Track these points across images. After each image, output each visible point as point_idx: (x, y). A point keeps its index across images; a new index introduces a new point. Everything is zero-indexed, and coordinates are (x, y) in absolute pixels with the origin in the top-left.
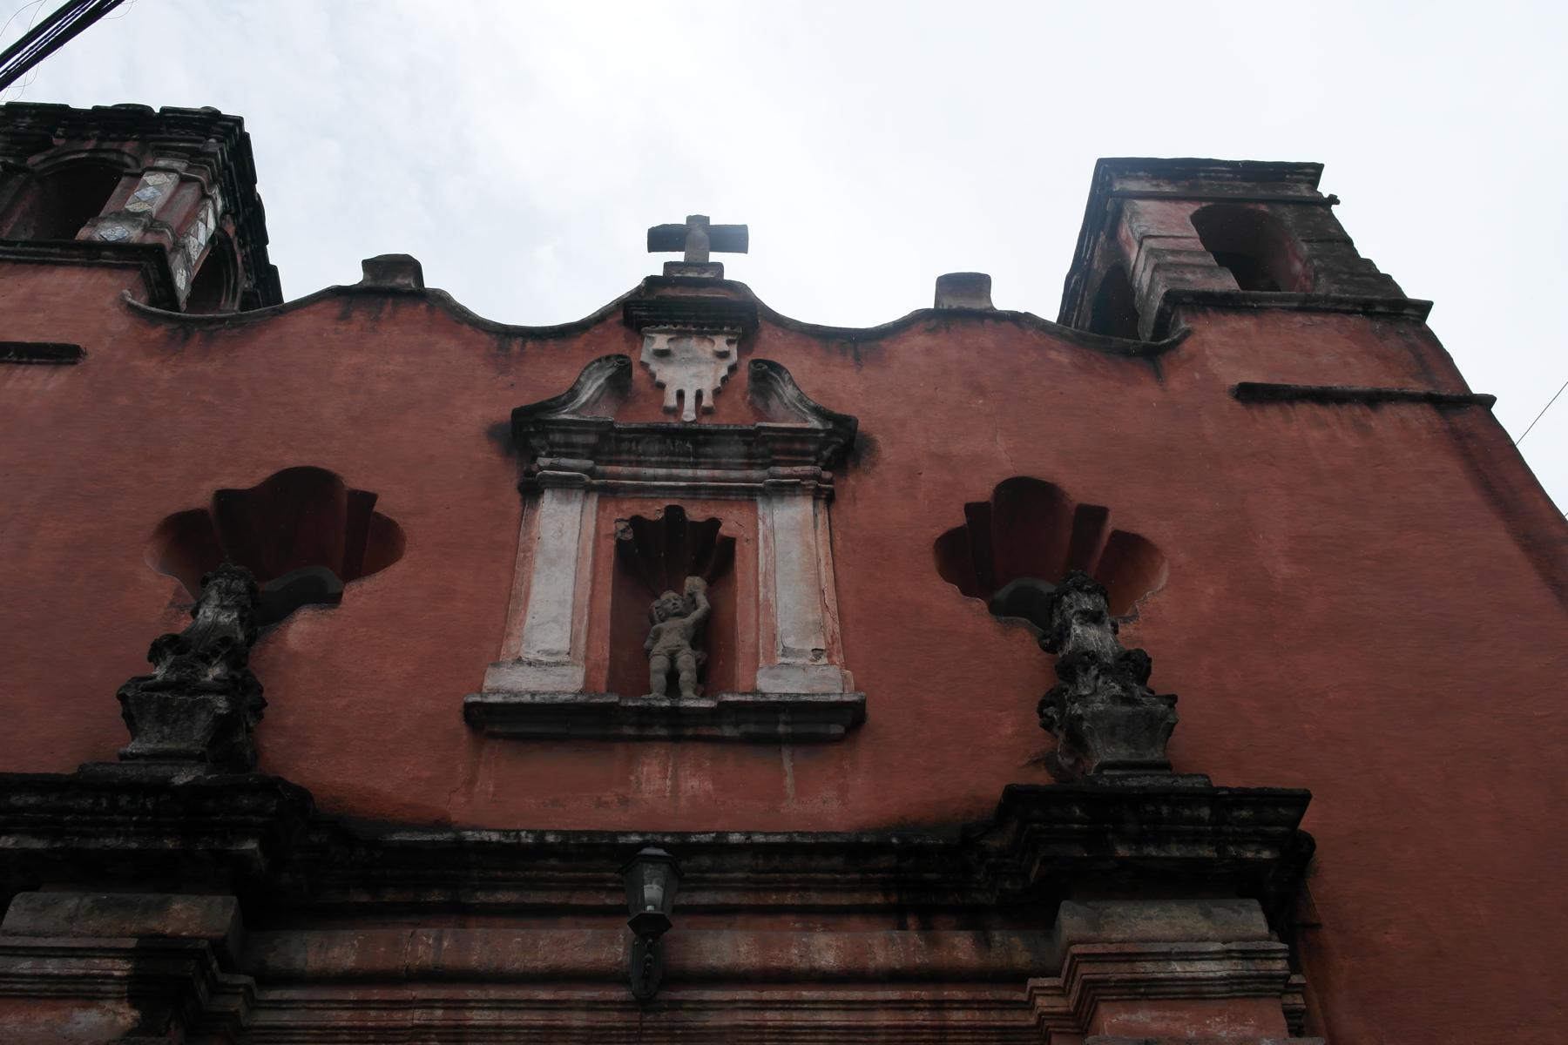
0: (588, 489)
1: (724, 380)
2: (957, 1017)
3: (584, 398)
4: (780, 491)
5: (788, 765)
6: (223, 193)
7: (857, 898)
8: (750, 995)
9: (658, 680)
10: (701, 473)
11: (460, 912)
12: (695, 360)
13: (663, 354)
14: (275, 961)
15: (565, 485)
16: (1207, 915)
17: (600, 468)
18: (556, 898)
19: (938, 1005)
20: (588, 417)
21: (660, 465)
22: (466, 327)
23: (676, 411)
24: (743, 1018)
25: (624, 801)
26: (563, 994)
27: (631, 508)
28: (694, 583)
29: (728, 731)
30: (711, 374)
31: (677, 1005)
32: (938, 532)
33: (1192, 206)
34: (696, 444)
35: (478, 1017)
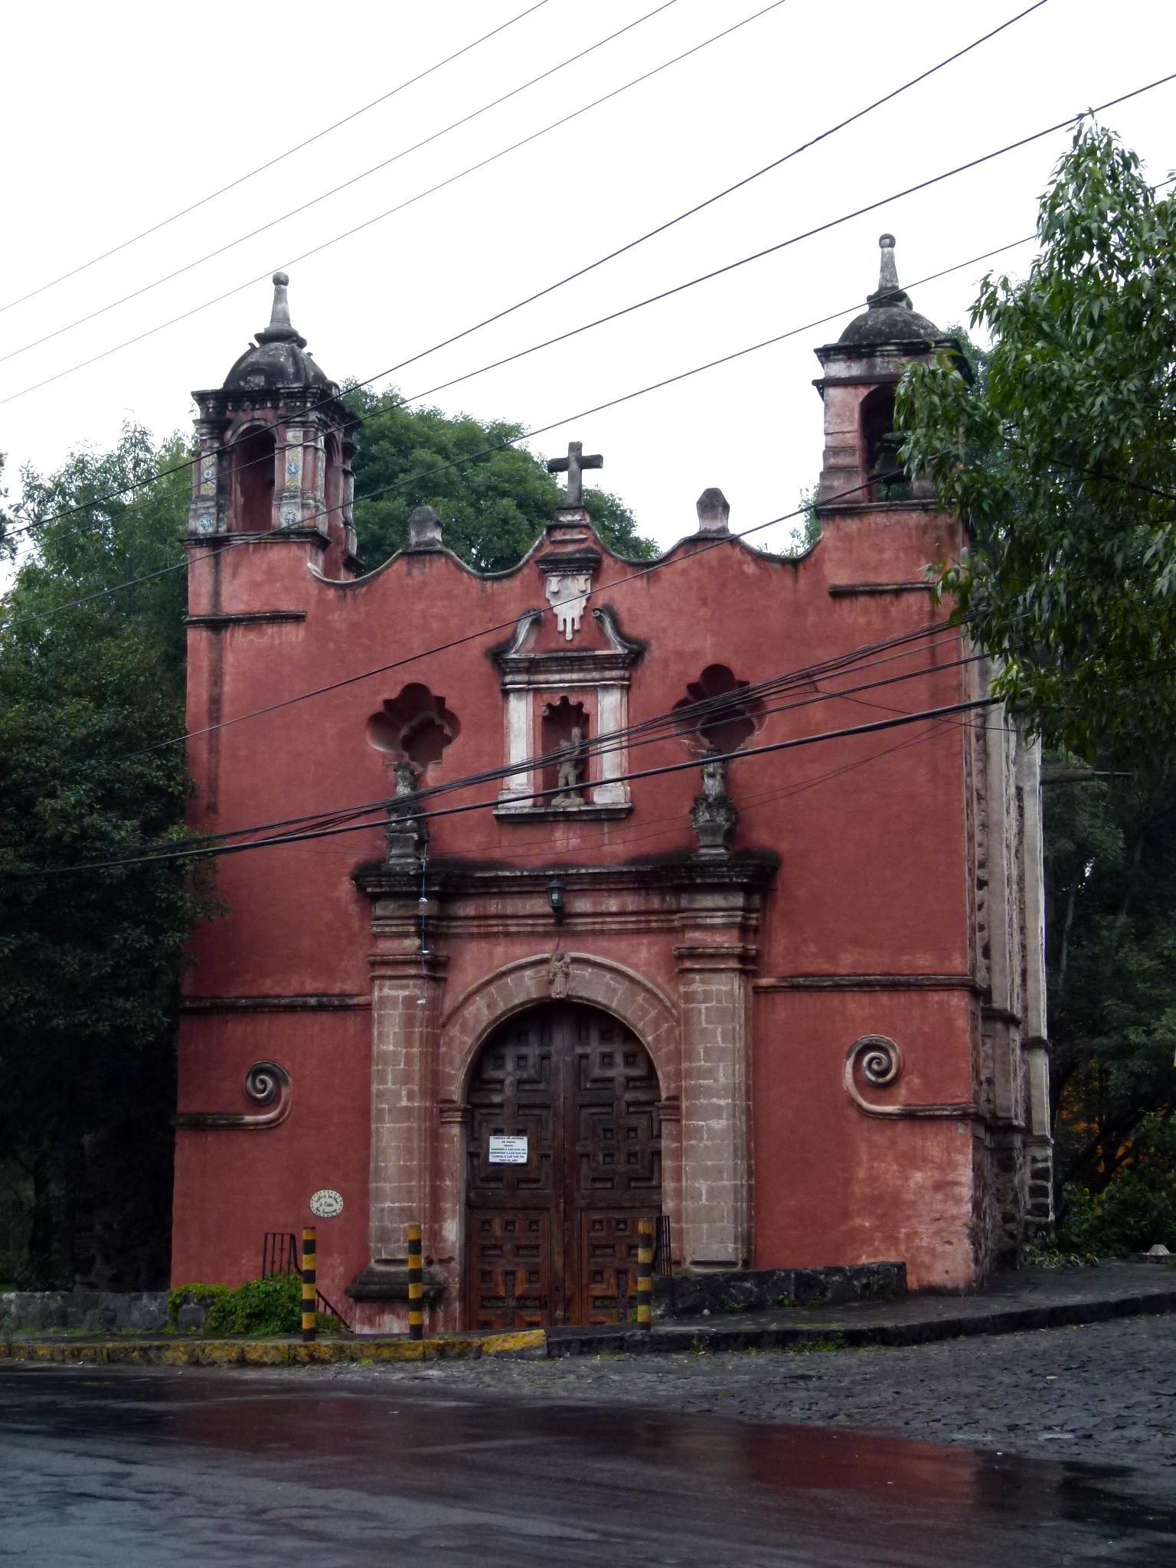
0: (529, 690)
1: (585, 608)
2: (654, 925)
3: (521, 640)
4: (606, 688)
5: (606, 830)
8: (590, 920)
10: (575, 676)
11: (501, 894)
13: (555, 593)
16: (725, 899)
18: (530, 889)
19: (648, 922)
22: (465, 575)
23: (564, 632)
24: (590, 927)
26: (536, 922)
27: (546, 698)
28: (576, 731)
30: (578, 606)
34: (571, 662)
35: (513, 929)
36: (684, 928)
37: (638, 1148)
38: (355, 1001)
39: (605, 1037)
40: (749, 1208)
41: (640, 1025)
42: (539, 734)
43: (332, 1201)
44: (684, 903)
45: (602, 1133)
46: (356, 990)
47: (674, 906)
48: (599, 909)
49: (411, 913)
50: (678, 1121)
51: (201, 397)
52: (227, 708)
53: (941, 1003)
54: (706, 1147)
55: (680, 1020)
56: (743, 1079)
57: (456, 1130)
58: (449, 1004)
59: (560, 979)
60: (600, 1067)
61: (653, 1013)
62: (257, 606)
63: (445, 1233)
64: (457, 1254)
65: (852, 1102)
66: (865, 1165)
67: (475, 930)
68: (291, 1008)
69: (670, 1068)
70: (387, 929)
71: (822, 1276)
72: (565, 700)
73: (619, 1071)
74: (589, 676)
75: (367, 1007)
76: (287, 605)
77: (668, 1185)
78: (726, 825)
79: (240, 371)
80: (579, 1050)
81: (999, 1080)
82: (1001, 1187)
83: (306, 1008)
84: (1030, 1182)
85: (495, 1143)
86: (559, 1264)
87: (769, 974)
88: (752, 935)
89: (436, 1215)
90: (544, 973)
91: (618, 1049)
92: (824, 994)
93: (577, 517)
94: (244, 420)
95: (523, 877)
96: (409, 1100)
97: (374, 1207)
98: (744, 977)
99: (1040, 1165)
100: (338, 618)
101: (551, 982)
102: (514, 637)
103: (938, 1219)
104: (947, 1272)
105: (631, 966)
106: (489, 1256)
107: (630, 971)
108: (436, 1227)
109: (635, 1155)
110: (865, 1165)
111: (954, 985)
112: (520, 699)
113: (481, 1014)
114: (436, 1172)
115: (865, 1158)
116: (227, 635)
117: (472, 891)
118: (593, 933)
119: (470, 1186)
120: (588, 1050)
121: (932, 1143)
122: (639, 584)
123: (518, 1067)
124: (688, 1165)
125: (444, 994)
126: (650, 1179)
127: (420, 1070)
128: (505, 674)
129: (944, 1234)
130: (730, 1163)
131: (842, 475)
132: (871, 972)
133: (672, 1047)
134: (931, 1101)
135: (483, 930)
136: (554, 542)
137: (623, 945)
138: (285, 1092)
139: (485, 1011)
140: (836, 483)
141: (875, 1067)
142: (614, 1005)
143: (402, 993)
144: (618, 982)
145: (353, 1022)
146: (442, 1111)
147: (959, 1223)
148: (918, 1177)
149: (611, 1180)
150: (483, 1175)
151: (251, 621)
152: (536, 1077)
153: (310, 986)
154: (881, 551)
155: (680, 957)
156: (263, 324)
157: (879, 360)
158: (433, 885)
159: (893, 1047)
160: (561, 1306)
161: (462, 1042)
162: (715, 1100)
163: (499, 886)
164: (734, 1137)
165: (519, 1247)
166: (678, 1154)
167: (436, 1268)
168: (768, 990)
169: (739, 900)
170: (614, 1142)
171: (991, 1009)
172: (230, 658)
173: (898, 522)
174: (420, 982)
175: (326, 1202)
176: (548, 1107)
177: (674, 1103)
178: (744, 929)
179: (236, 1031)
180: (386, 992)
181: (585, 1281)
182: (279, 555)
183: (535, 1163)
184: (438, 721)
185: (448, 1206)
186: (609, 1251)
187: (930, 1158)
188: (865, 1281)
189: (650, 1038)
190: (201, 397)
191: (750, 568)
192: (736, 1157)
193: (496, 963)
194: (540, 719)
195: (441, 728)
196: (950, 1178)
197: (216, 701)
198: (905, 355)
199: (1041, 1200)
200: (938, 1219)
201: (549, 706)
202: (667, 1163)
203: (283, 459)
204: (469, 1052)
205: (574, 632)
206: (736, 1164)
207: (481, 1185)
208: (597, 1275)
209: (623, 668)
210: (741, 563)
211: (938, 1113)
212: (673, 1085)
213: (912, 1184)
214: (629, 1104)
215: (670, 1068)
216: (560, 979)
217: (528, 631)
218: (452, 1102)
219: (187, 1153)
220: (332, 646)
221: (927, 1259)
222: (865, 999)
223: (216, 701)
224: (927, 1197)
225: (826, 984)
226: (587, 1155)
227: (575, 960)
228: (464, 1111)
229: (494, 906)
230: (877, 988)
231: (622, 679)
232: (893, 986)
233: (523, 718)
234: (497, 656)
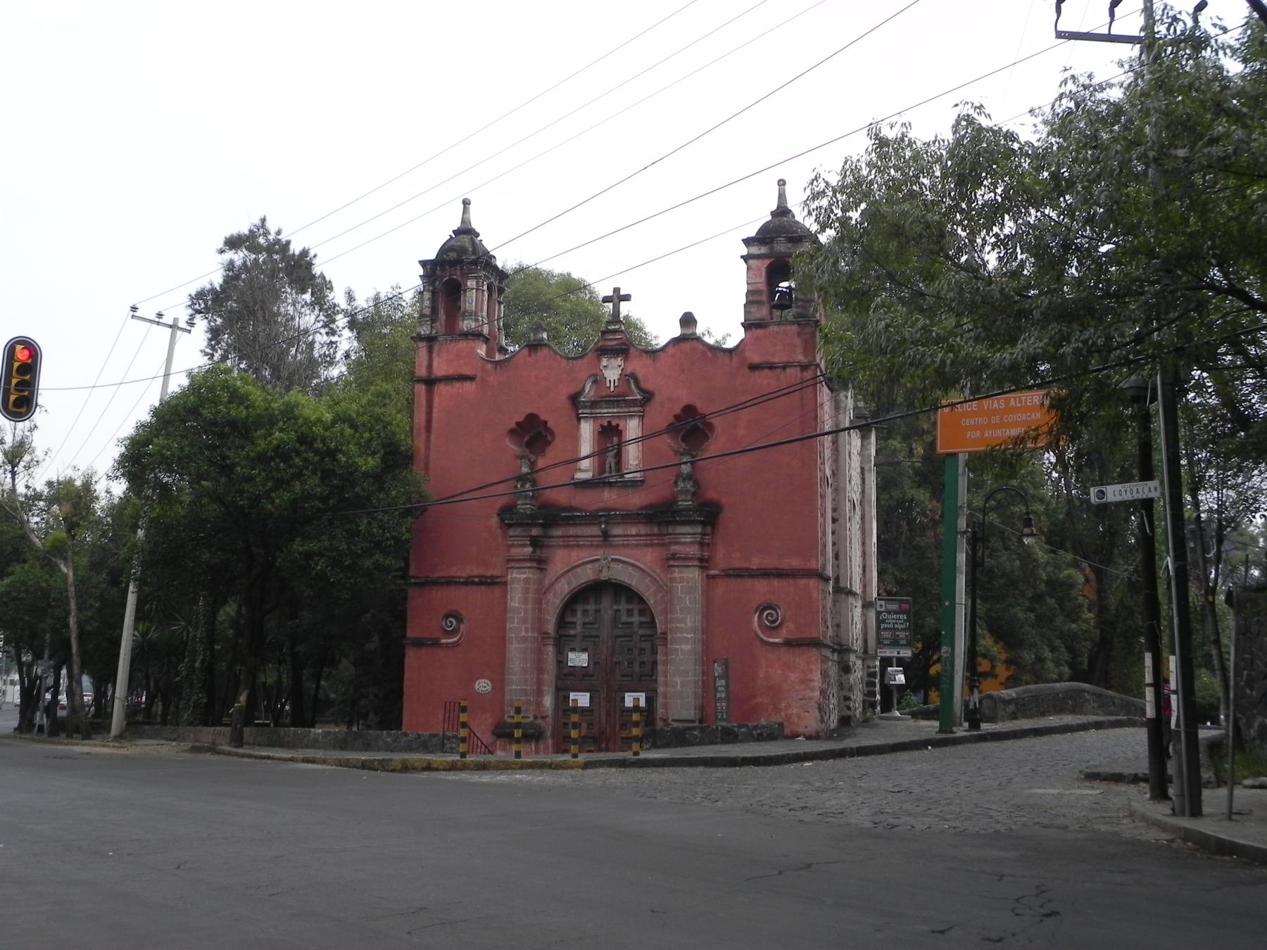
2: (655, 542)
4: (631, 416)
9: (608, 469)
10: (615, 410)
11: (575, 525)
12: (613, 368)
14: (549, 534)
17: (593, 411)
21: (606, 408)
24: (621, 543)
27: (600, 421)
35: (581, 543)
36: (670, 544)
37: (645, 659)
38: (499, 580)
39: (629, 600)
41: (647, 595)
44: (670, 530)
46: (499, 574)
47: (665, 532)
48: (625, 533)
49: (527, 534)
50: (666, 645)
51: (424, 263)
55: (667, 591)
58: (547, 582)
59: (605, 570)
63: (544, 703)
64: (550, 714)
65: (758, 636)
67: (561, 543)
69: (662, 617)
70: (516, 542)
72: (609, 422)
73: (636, 619)
74: (622, 411)
75: (505, 583)
77: (661, 679)
78: (693, 489)
79: (444, 250)
80: (615, 607)
81: (843, 625)
83: (473, 583)
84: (866, 679)
85: (571, 655)
87: (715, 569)
88: (706, 548)
89: (539, 693)
90: (597, 566)
91: (635, 607)
93: (617, 327)
95: (586, 516)
96: (526, 631)
97: (506, 689)
99: (872, 670)
101: (601, 571)
102: (583, 390)
105: (642, 563)
108: (540, 699)
109: (644, 663)
112: (586, 422)
113: (564, 588)
114: (540, 670)
117: (560, 522)
119: (558, 677)
120: (620, 607)
121: (799, 659)
122: (649, 362)
124: (671, 668)
126: (652, 676)
128: (579, 409)
133: (664, 606)
135: (566, 543)
138: (462, 627)
139: (566, 586)
141: (770, 618)
142: (633, 584)
143: (525, 576)
145: (497, 590)
148: (793, 676)
149: (631, 676)
150: (565, 672)
151: (449, 379)
153: (476, 572)
155: (668, 559)
156: (457, 224)
160: (605, 742)
161: (555, 602)
166: (666, 663)
168: (714, 577)
169: (699, 529)
171: (839, 587)
172: (436, 400)
174: (532, 570)
175: (483, 685)
176: (598, 637)
177: (663, 636)
178: (701, 544)
180: (515, 575)
181: (617, 729)
182: (463, 344)
184: (544, 433)
185: (546, 688)
188: (759, 731)
189: (652, 602)
190: (424, 263)
192: (695, 665)
193: (572, 561)
194: (596, 433)
195: (546, 437)
197: (429, 422)
199: (872, 689)
201: (601, 426)
202: (660, 668)
203: (465, 296)
205: (615, 387)
209: (640, 406)
212: (663, 627)
214: (641, 636)
215: (662, 617)
219: (412, 658)
221: (796, 720)
222: (765, 582)
223: (429, 422)
226: (619, 663)
227: (613, 560)
228: (555, 638)
229: (572, 531)
231: (640, 412)
232: (780, 574)
233: (588, 433)
234: (574, 399)
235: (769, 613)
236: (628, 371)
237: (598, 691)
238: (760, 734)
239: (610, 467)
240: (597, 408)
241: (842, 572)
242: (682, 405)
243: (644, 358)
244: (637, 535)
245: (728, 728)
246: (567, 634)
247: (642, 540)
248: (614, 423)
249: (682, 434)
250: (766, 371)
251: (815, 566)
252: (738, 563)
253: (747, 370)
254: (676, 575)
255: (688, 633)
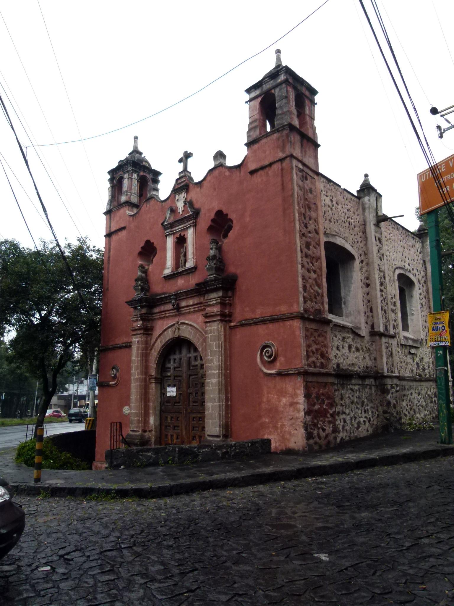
0: (171, 234)
4: (189, 227)
6: (135, 173)
7: (194, 295)
8: (186, 309)
10: (182, 226)
11: (165, 303)
15: (169, 235)
20: (168, 223)
23: (180, 212)
24: (186, 311)
25: (177, 285)
29: (185, 273)
31: (181, 311)
32: (207, 228)
33: (266, 89)
35: (168, 315)
40: (227, 414)
42: (174, 248)
43: (127, 410)
45: (195, 385)
52: (111, 259)
53: (290, 325)
54: (211, 390)
55: (205, 340)
56: (223, 363)
57: (153, 385)
60: (194, 361)
61: (201, 340)
62: (117, 228)
66: (266, 396)
67: (159, 317)
68: (121, 347)
71: (196, 449)
72: (180, 234)
76: (123, 226)
80: (188, 355)
81: (378, 359)
82: (381, 400)
85: (169, 389)
86: (184, 433)
89: (146, 414)
92: (252, 326)
94: (117, 177)
95: (167, 296)
98: (224, 323)
100: (132, 225)
101: (175, 331)
102: (166, 218)
103: (291, 419)
104: (295, 443)
106: (168, 429)
107: (195, 325)
110: (266, 396)
111: (294, 317)
113: (159, 345)
115: (266, 393)
116: (112, 238)
117: (158, 304)
118: (187, 313)
119: (162, 404)
120: (191, 355)
122: (198, 190)
123: (174, 362)
125: (151, 340)
127: (141, 365)
129: (294, 425)
130: (218, 396)
131: (253, 130)
132: (266, 316)
134: (288, 368)
136: (178, 184)
137: (194, 316)
140: (251, 134)
141: (267, 354)
142: (191, 338)
144: (192, 330)
146: (150, 379)
147: (299, 420)
148: (284, 400)
149: (197, 402)
152: (178, 366)
154: (265, 152)
156: (131, 150)
157: (264, 86)
158: (143, 303)
159: (273, 346)
161: (154, 354)
162: (213, 371)
163: (163, 301)
164: (219, 386)
165: (175, 427)
167: (146, 434)
168: (234, 327)
169: (220, 294)
170: (198, 388)
171: (374, 331)
172: (112, 244)
173: (270, 139)
174: (141, 335)
178: (223, 304)
179: (111, 355)
183: (178, 397)
186: (197, 429)
187: (288, 392)
188: (224, 451)
189: (200, 349)
191: (227, 173)
192: (219, 393)
196: (295, 400)
198: (272, 80)
200: (291, 419)
204: (156, 358)
206: (220, 397)
207: (167, 404)
208: (194, 438)
209: (194, 219)
210: (225, 172)
211: (289, 372)
213: (282, 404)
216: (177, 330)
217: (170, 214)
218: (152, 376)
220: (131, 234)
221: (288, 436)
222: (264, 327)
224: (287, 409)
225: (251, 322)
227: (182, 323)
229: (163, 308)
230: (268, 322)
232: (274, 320)
235: (267, 351)
236: (188, 200)
237: (181, 413)
238: (227, 452)
239: (182, 263)
240: (174, 227)
241: (375, 320)
242: (215, 212)
243: (196, 188)
244: (193, 305)
245: (187, 449)
246: (166, 375)
247: (196, 308)
248: (182, 235)
249: (223, 233)
250: (261, 172)
251: (296, 309)
252: (249, 315)
253: (249, 174)
254: (208, 328)
255: (215, 370)
